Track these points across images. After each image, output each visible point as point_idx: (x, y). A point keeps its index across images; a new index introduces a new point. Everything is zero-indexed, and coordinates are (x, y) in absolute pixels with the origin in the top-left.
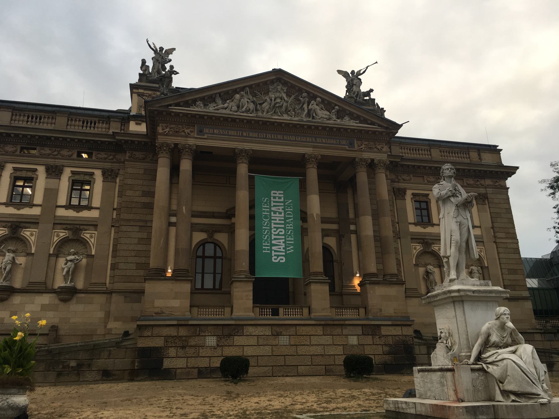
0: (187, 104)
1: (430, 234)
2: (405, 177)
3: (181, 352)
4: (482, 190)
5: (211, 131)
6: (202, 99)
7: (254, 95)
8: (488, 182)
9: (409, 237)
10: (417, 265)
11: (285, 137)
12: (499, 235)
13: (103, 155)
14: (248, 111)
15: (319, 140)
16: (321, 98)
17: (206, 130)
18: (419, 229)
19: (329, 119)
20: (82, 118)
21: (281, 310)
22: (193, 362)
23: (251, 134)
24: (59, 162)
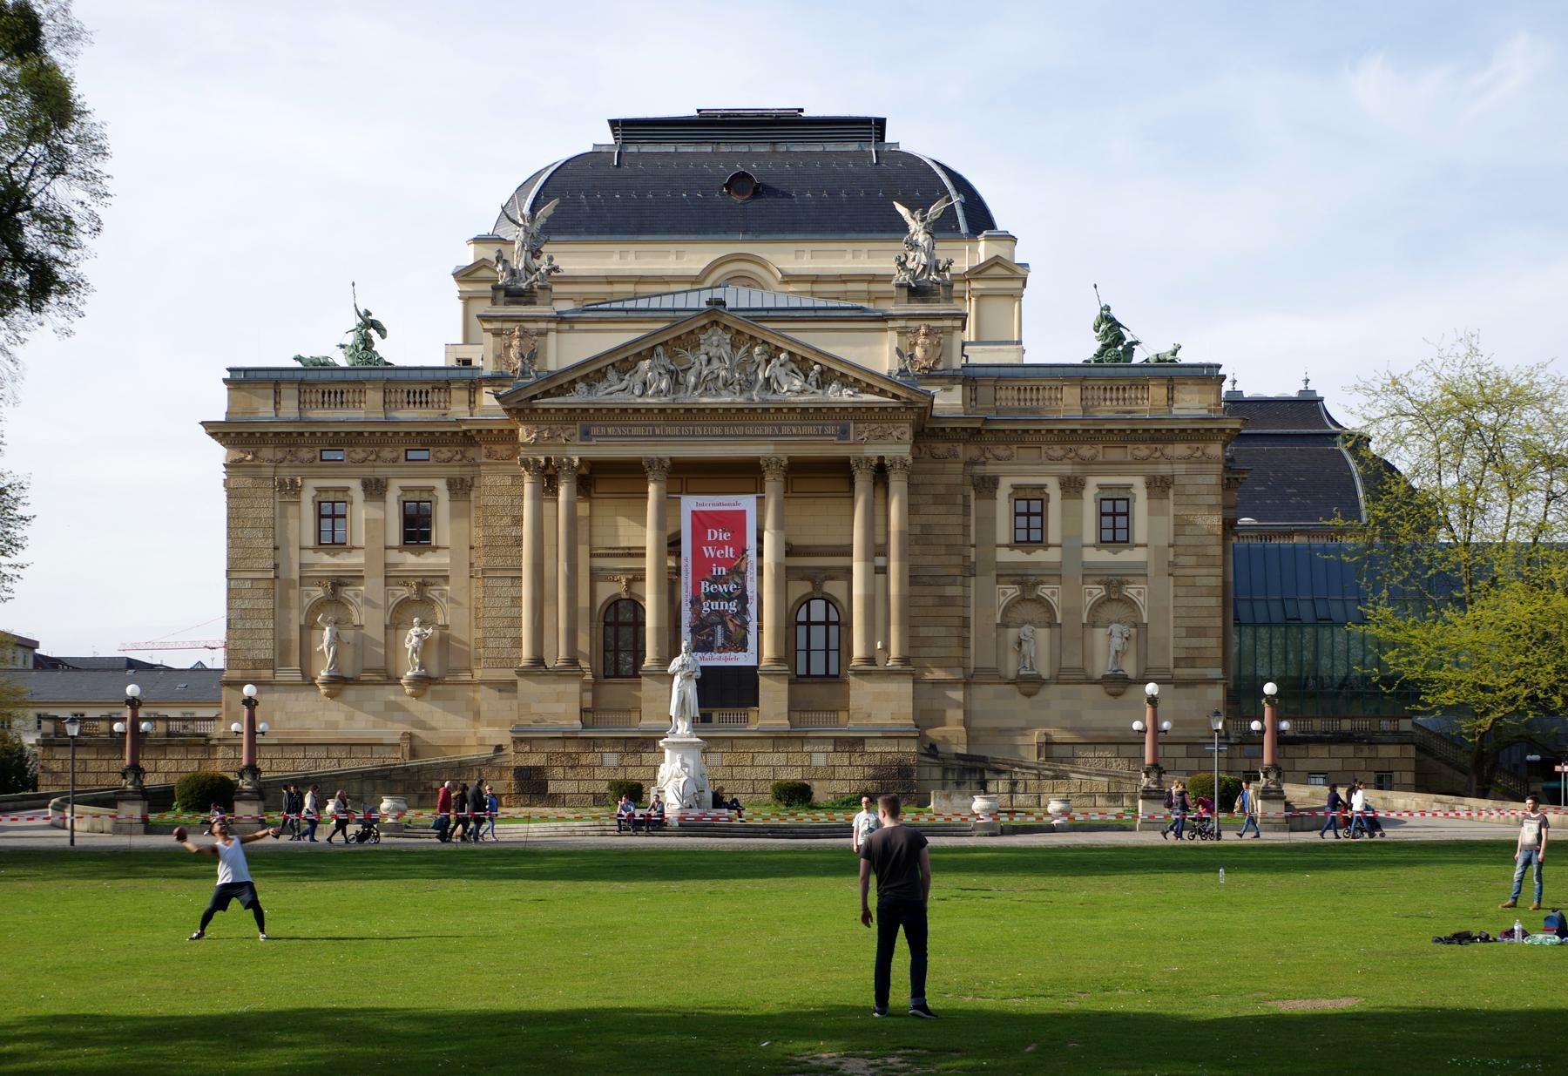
0: (562, 390)
1: (1037, 564)
2: (1001, 451)
3: (570, 774)
4: (1164, 469)
5: (603, 430)
6: (585, 378)
7: (673, 356)
8: (1180, 449)
9: (994, 573)
10: (1004, 625)
11: (727, 430)
12: (1183, 560)
13: (445, 453)
14: (659, 392)
15: (785, 430)
16: (790, 353)
17: (595, 431)
18: (1018, 556)
19: (802, 392)
20: (406, 388)
21: (715, 716)
22: (585, 787)
23: (668, 430)
24: (380, 472)
